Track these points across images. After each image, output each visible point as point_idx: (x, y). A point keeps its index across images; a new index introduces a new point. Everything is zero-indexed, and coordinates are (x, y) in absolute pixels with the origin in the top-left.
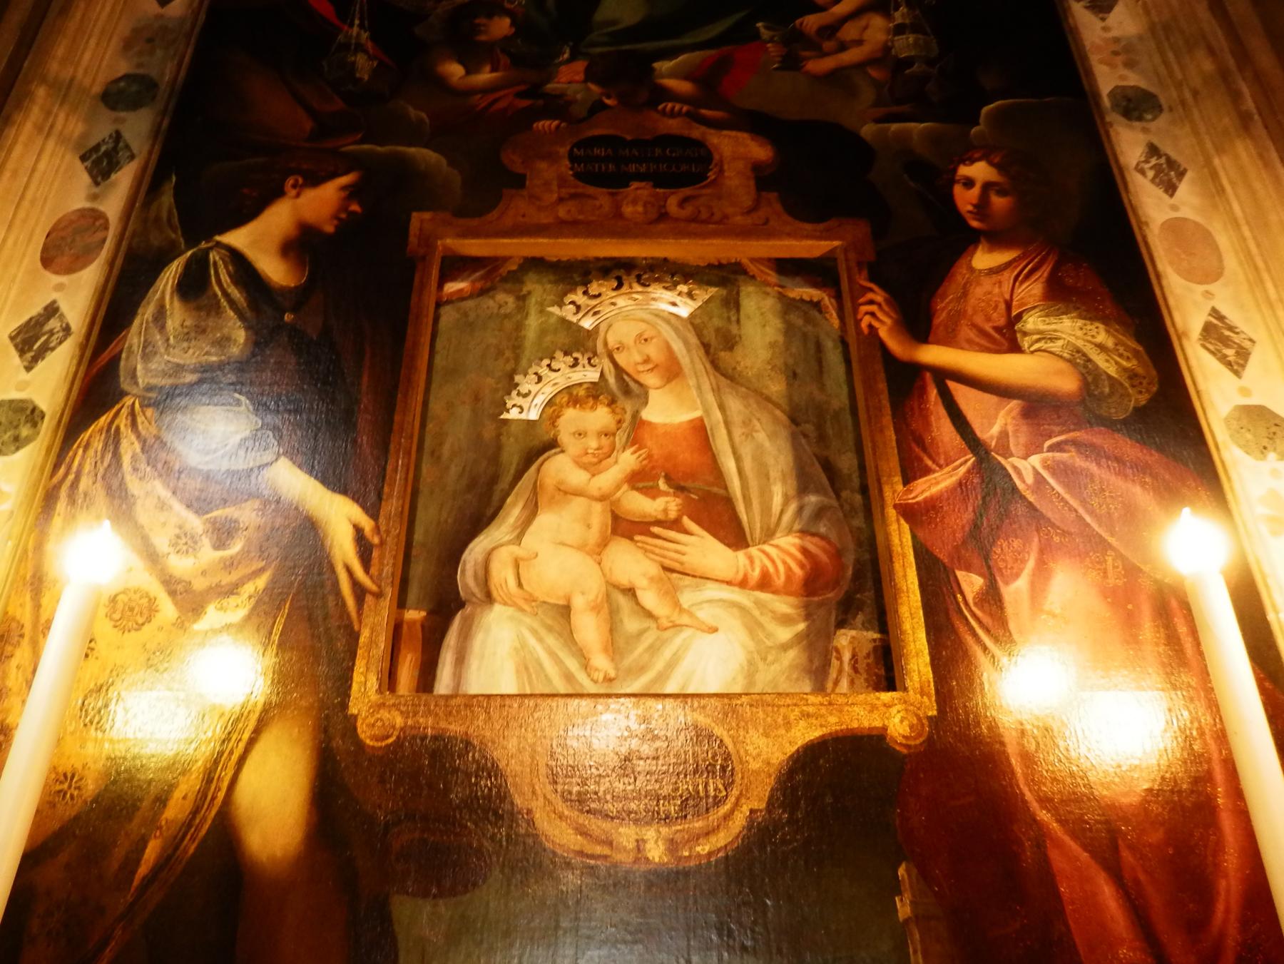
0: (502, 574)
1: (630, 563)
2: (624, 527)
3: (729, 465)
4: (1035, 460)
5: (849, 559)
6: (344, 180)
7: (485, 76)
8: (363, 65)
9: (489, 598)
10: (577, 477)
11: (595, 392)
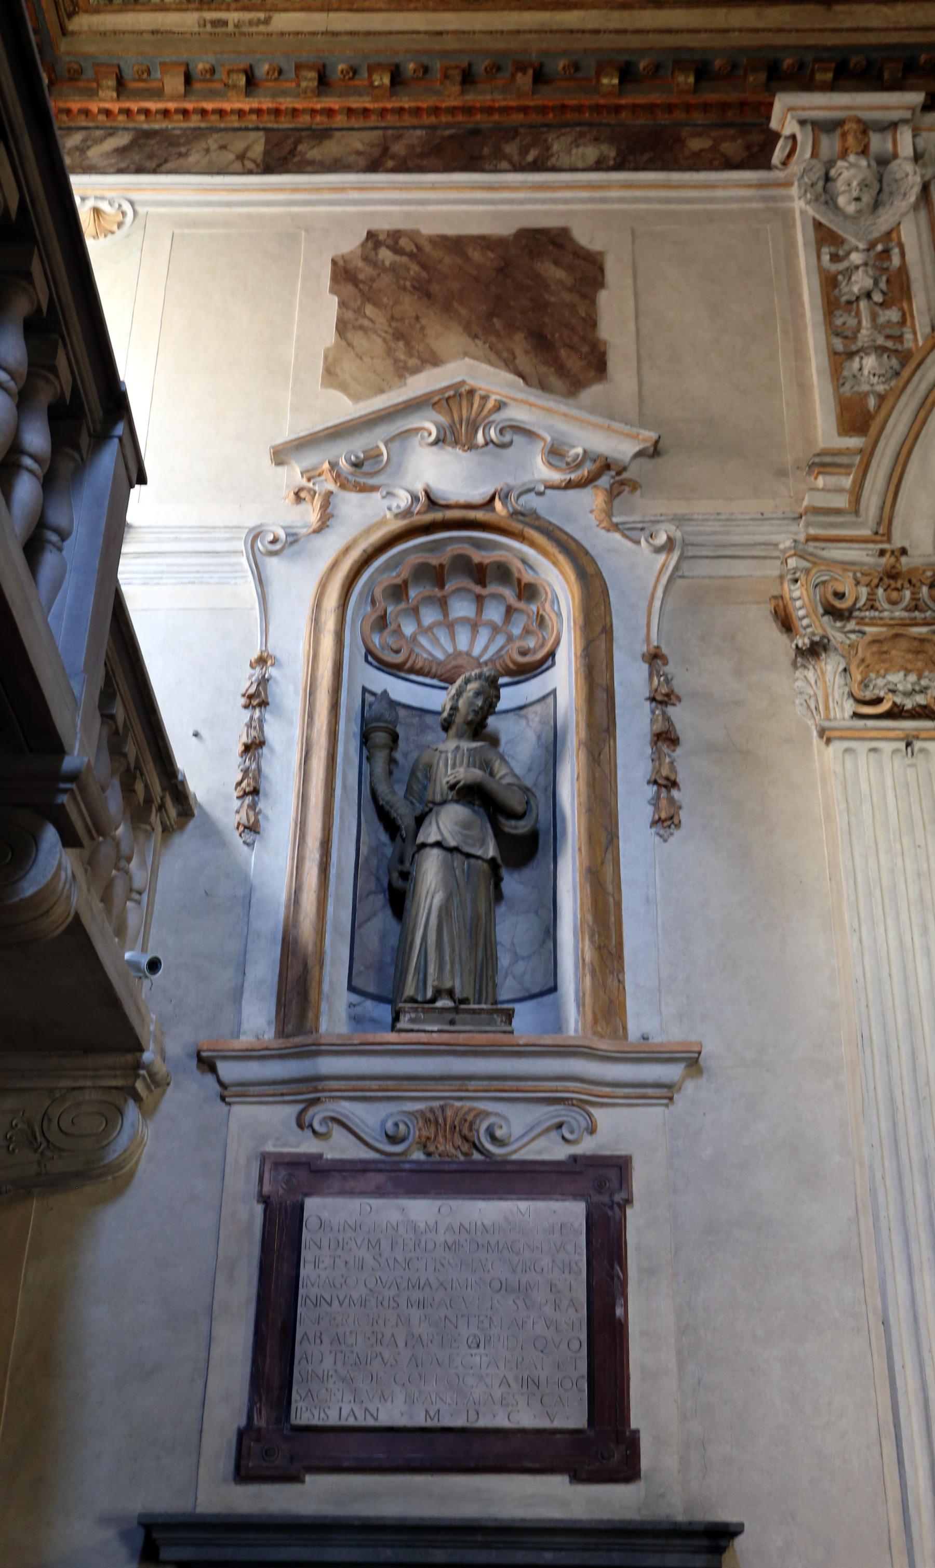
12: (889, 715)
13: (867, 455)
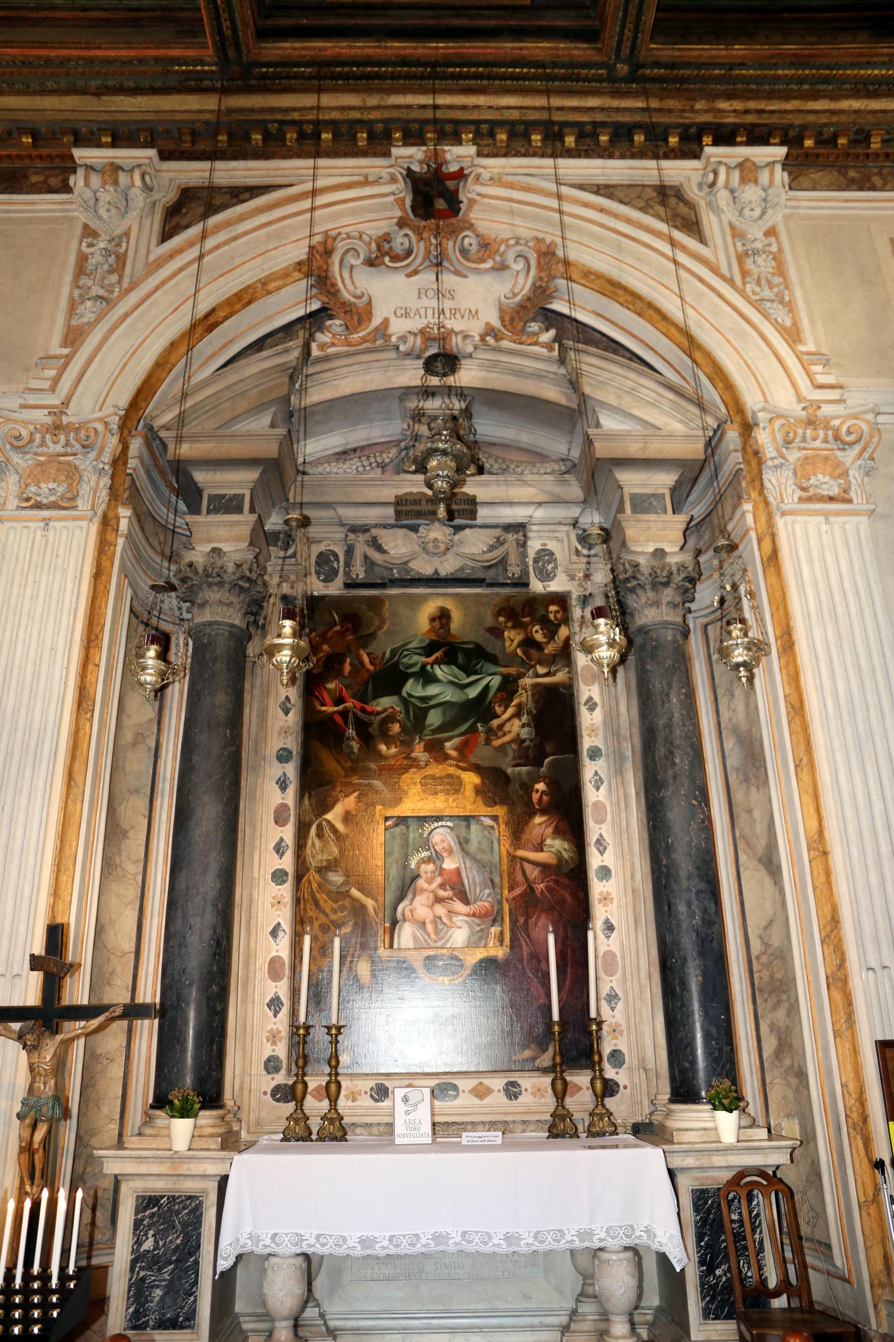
0: (408, 914)
1: (440, 910)
2: (438, 900)
3: (466, 881)
4: (542, 885)
5: (496, 908)
6: (356, 794)
7: (393, 750)
8: (355, 746)
9: (405, 920)
10: (426, 886)
11: (429, 860)
12: (32, 507)
13: (69, 358)
